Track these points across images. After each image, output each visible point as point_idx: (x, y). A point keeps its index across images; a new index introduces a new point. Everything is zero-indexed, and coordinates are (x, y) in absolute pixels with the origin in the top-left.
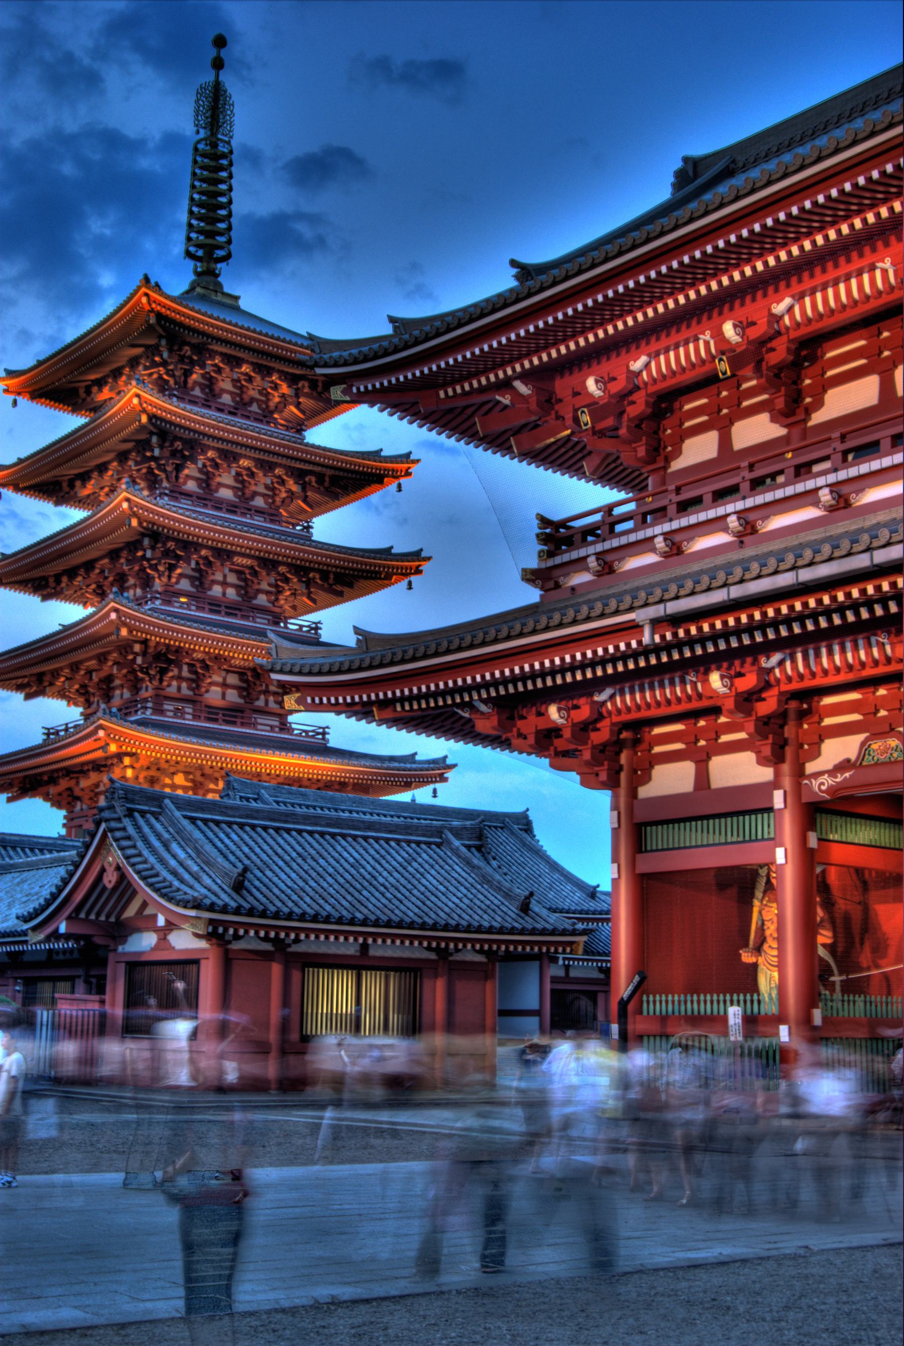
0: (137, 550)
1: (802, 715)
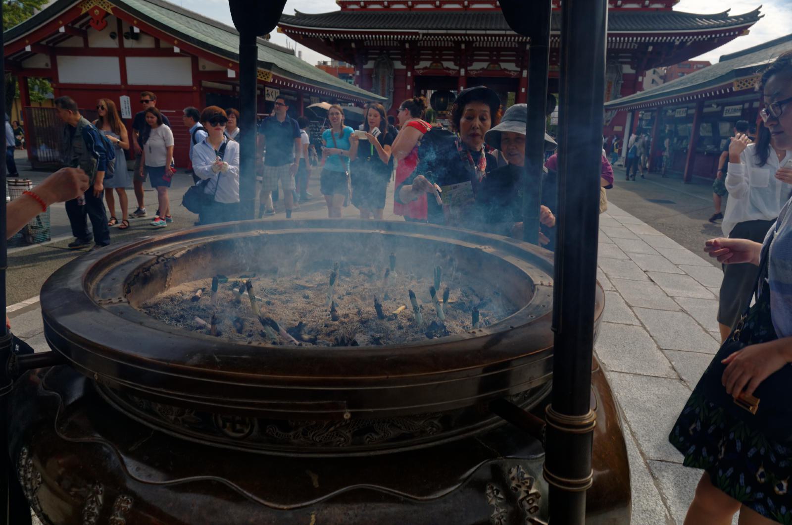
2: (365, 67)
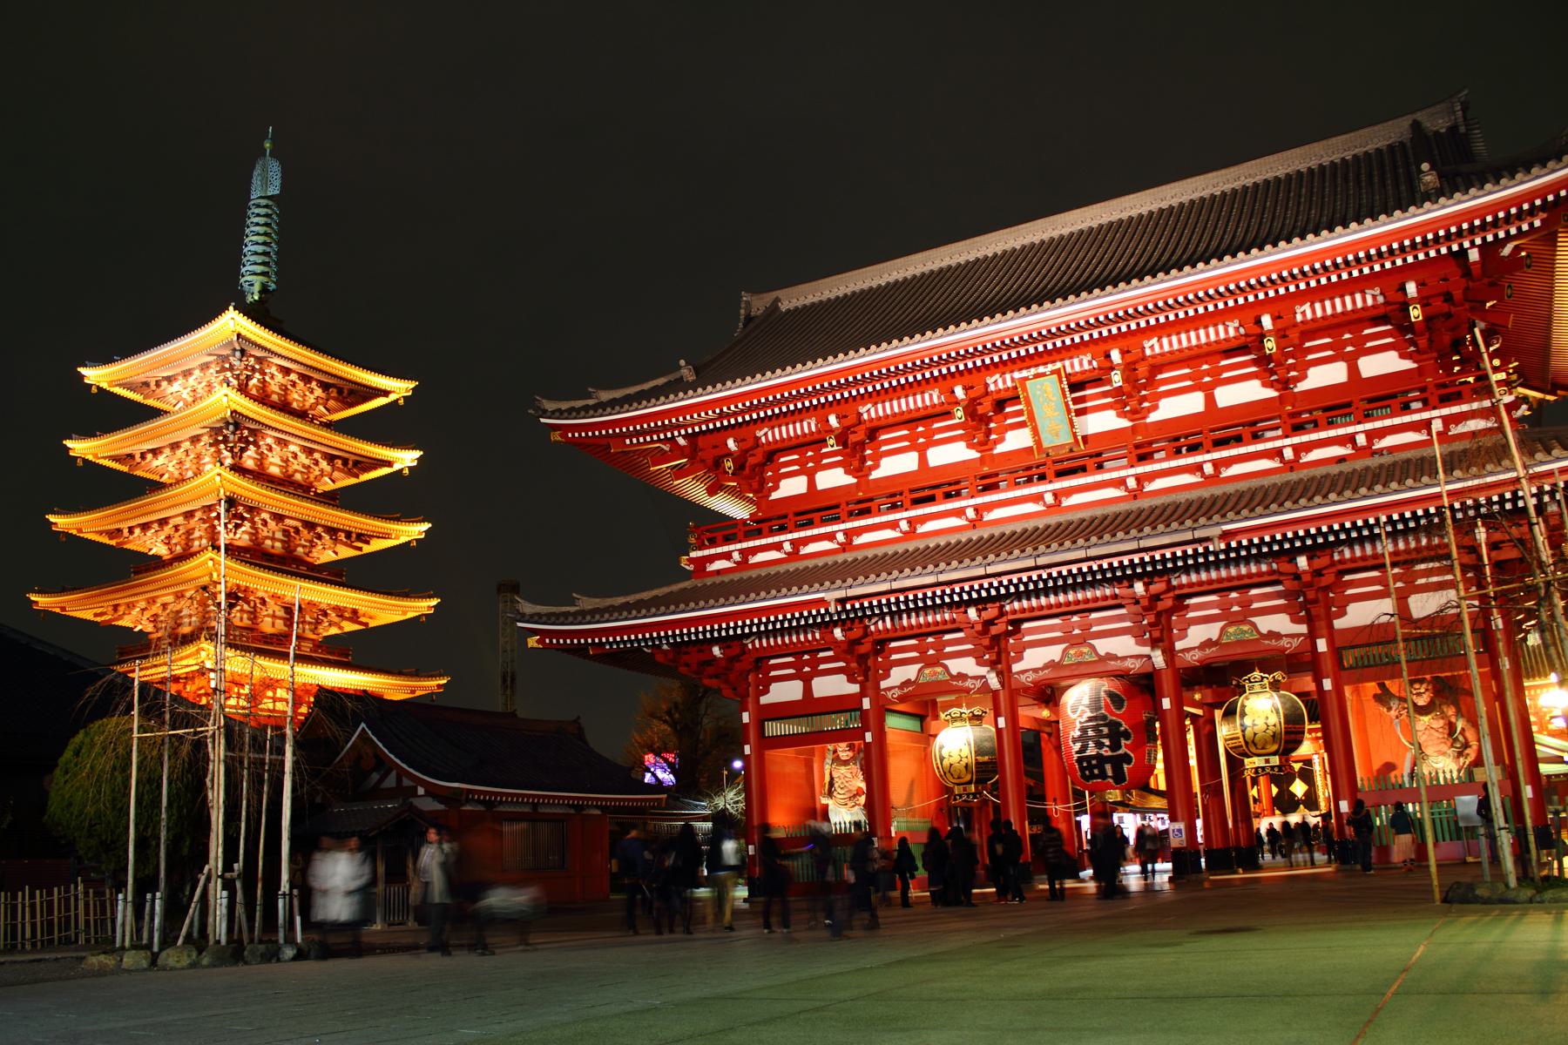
1: (878, 653)
2: (764, 700)
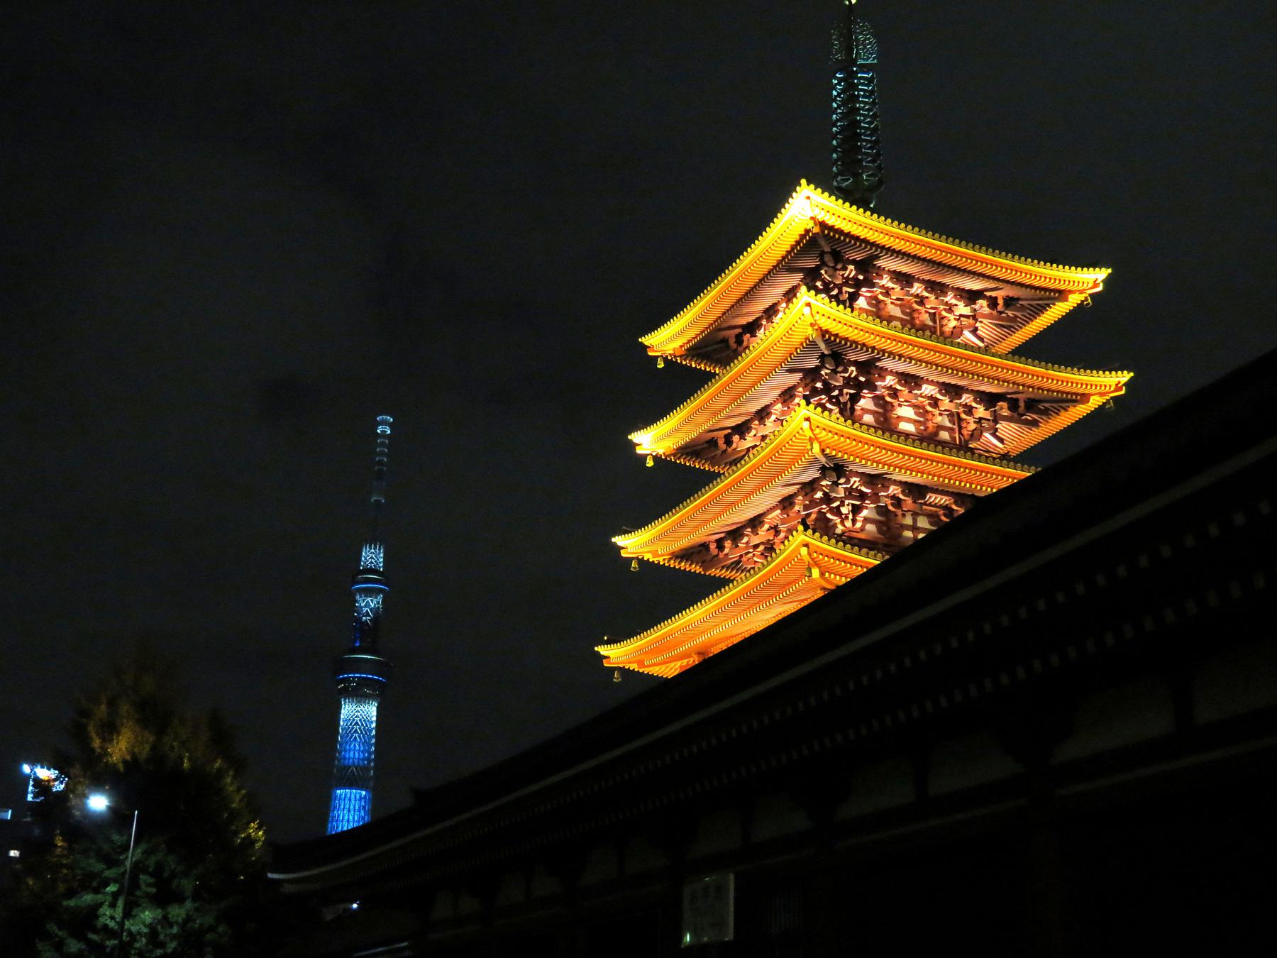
0: (814, 491)
